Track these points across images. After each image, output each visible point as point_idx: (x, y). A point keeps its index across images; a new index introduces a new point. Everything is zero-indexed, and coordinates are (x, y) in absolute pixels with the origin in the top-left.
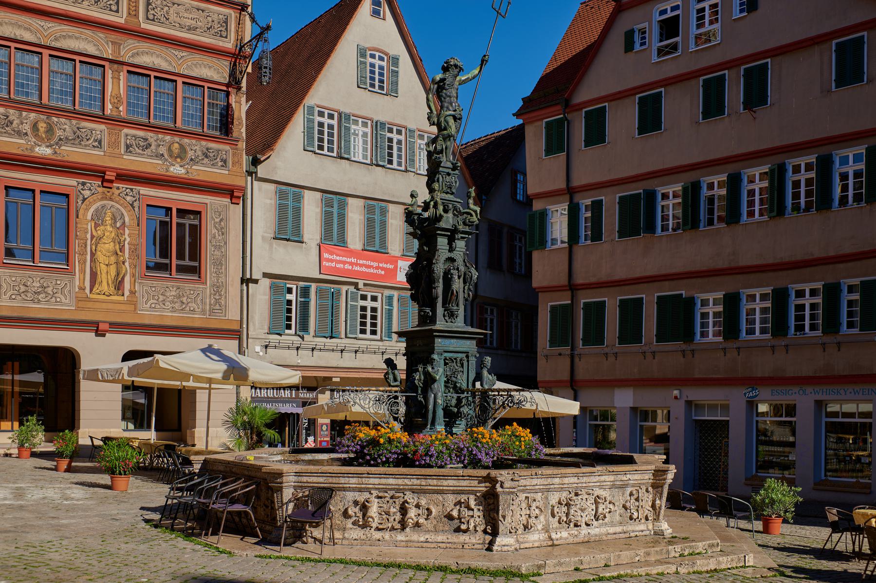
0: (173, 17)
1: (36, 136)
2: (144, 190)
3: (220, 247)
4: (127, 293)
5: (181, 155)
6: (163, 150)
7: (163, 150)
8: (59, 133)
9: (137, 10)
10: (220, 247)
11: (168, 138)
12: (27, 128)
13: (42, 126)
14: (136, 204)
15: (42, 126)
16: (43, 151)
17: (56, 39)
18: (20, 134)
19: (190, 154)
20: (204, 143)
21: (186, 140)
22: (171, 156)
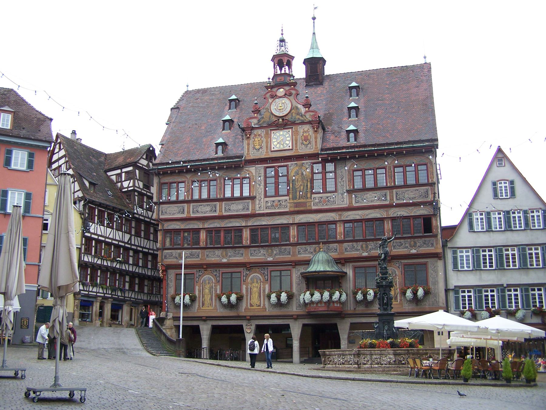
0: (406, 196)
1: (362, 250)
2: (403, 261)
3: (435, 278)
4: (399, 300)
5: (414, 246)
6: (407, 245)
7: (407, 245)
8: (370, 247)
9: (393, 198)
10: (435, 278)
11: (409, 240)
12: (359, 247)
13: (364, 246)
14: (400, 267)
15: (364, 246)
16: (365, 254)
17: (367, 215)
18: (357, 250)
19: (418, 244)
20: (423, 239)
21: (416, 239)
22: (411, 247)
